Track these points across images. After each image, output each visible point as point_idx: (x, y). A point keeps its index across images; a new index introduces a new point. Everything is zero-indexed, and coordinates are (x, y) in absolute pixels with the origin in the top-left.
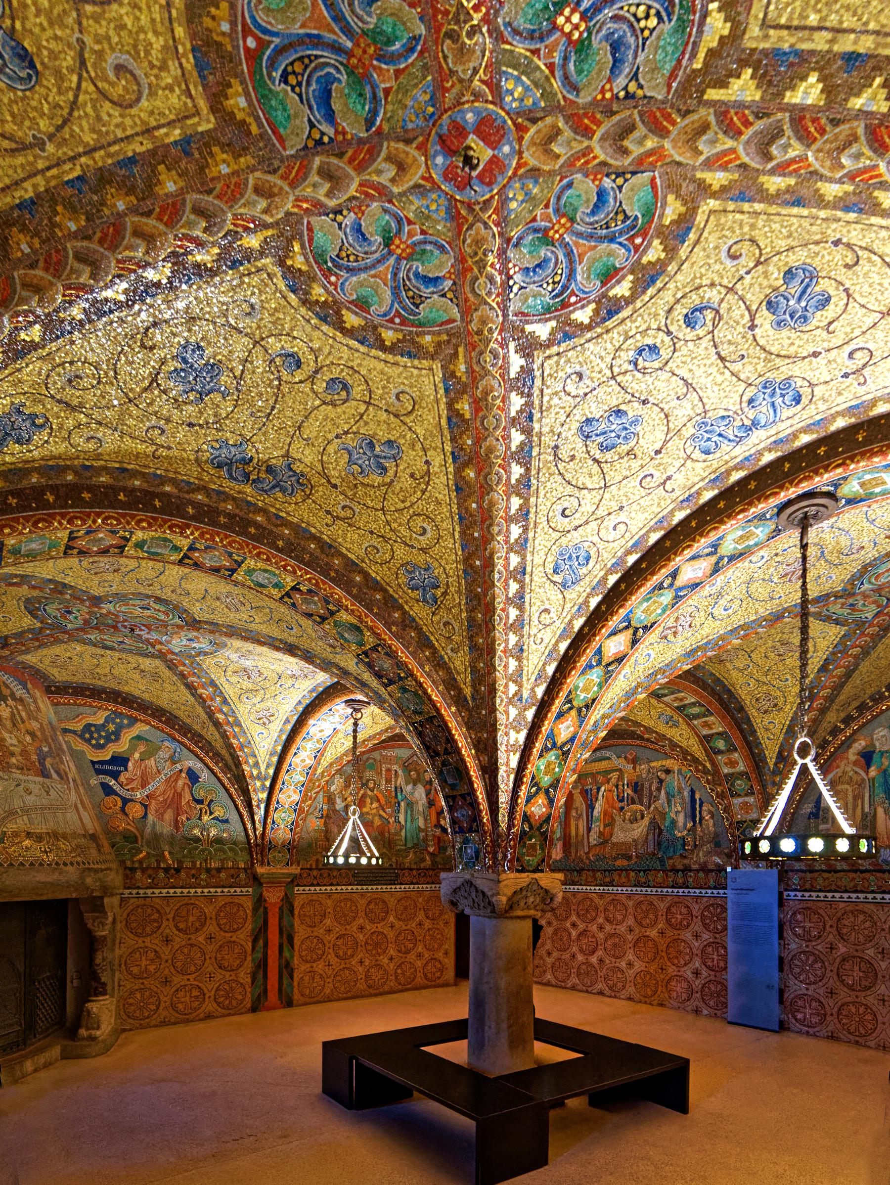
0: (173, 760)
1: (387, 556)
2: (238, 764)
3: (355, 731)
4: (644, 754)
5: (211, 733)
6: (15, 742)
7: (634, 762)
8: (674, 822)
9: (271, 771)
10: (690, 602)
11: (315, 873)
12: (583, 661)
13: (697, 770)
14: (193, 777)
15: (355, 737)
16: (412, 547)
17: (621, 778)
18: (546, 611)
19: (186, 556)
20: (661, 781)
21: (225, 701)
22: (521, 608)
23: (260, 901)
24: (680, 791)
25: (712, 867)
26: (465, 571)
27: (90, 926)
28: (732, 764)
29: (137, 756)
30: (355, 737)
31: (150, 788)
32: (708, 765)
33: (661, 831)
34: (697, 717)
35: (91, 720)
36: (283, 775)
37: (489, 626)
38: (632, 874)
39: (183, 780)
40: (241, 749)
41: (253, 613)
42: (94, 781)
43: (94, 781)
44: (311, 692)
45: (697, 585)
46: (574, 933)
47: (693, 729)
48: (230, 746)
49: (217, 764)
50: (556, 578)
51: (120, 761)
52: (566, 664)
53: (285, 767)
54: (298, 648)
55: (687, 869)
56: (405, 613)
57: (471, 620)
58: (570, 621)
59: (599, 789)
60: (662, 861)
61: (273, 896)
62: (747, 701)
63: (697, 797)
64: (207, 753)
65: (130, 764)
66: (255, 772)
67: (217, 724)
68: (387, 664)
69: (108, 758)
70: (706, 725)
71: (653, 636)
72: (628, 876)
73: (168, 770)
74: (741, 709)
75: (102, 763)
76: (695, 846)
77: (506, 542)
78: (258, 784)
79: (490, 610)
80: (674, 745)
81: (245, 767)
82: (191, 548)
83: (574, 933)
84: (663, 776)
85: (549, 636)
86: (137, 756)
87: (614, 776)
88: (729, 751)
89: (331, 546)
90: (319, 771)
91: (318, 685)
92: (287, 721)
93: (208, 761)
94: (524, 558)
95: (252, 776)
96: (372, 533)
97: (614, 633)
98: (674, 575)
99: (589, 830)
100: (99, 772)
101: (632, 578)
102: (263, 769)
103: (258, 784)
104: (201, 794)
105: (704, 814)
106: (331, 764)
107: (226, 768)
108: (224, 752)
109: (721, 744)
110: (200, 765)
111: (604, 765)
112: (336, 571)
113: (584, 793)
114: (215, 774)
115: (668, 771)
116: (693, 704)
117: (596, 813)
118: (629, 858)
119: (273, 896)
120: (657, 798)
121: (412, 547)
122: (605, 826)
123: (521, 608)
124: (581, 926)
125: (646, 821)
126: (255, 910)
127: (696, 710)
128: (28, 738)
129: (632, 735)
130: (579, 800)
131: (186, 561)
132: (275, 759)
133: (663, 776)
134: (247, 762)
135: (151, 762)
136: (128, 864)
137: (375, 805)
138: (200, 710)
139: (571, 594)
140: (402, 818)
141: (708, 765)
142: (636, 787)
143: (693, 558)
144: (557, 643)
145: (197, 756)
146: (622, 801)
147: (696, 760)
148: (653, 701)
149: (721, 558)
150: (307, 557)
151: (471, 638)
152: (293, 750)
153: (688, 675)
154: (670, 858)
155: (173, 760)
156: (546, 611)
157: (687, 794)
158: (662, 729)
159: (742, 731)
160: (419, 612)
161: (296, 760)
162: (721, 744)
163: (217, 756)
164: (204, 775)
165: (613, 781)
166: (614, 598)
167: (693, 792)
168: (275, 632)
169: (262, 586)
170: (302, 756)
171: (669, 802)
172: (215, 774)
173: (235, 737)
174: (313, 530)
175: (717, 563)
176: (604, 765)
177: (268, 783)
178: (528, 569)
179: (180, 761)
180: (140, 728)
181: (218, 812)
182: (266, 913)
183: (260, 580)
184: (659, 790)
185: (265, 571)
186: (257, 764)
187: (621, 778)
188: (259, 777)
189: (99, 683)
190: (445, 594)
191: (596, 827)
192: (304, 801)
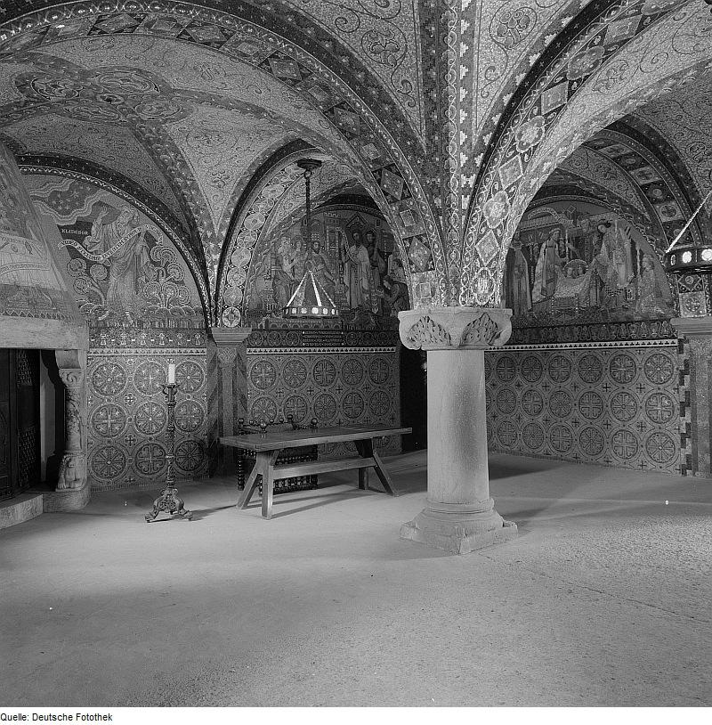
1: (354, 26)
2: (193, 227)
3: (308, 190)
4: (583, 208)
5: (169, 199)
7: (576, 216)
8: (616, 275)
9: (224, 233)
10: (619, 57)
11: (265, 334)
12: (524, 111)
13: (636, 221)
14: (151, 241)
15: (308, 195)
16: (377, 17)
17: (562, 233)
18: (493, 68)
19: (185, 32)
20: (601, 235)
21: (184, 165)
22: (470, 67)
23: (214, 361)
24: (621, 244)
25: (652, 317)
26: (422, 36)
27: (64, 380)
28: (670, 212)
29: (99, 221)
30: (308, 195)
31: (112, 251)
32: (646, 215)
33: (603, 284)
34: (634, 167)
35: (57, 188)
36: (236, 237)
37: (441, 83)
38: (576, 329)
39: (141, 244)
41: (226, 80)
42: (61, 246)
44: (264, 154)
45: (625, 41)
46: (519, 394)
47: (630, 179)
48: (185, 209)
50: (500, 40)
51: (84, 225)
52: (509, 114)
53: (238, 228)
54: (264, 110)
55: (629, 321)
56: (367, 73)
57: (427, 79)
58: (513, 76)
59: (540, 246)
60: (604, 313)
61: (227, 357)
62: (682, 150)
63: (638, 248)
64: (163, 217)
65: (93, 229)
66: (209, 234)
67: (175, 188)
68: (349, 119)
70: (642, 174)
71: (588, 88)
72: (571, 332)
74: (676, 159)
75: (67, 227)
76: (637, 297)
77: (458, 11)
78: (212, 245)
79: (443, 68)
80: (613, 197)
81: (200, 229)
82: (191, 26)
83: (519, 394)
84: (602, 229)
85: (495, 91)
86: (99, 221)
87: (555, 232)
88: (667, 200)
89: (306, 19)
90: (268, 232)
91: (272, 147)
92: (240, 183)
93: (164, 224)
94: (472, 24)
96: (342, 6)
97: (552, 85)
98: (603, 34)
99: (532, 287)
100: (65, 236)
101: (566, 37)
102: (216, 231)
103: (212, 245)
104: (157, 257)
105: (645, 264)
106: (280, 225)
107: (181, 232)
108: (181, 217)
109: (658, 194)
111: (544, 221)
112: (309, 40)
113: (526, 250)
114: (171, 238)
115: (608, 225)
116: (630, 154)
117: (538, 270)
118: (571, 313)
119: (227, 357)
120: (598, 252)
121: (377, 17)
122: (548, 282)
123: (470, 67)
124: (526, 386)
125: (588, 275)
126: (210, 371)
127: (631, 161)
128: (11, 202)
129: (573, 190)
130: (521, 258)
131: (184, 36)
132: (228, 221)
133: (602, 229)
134: (202, 224)
135: (112, 227)
136: (94, 324)
137: (320, 267)
138: (160, 176)
139: (513, 54)
140: (346, 280)
141: (646, 215)
142: (578, 241)
143: (619, 19)
144: (501, 96)
145: (154, 220)
146: (564, 256)
147: (634, 211)
148: (591, 153)
149: (645, 17)
150: (285, 29)
151: (426, 93)
152: (246, 212)
153: (618, 126)
154: (612, 310)
156: (493, 68)
157: (627, 245)
158: (601, 182)
159: (678, 180)
160: (380, 72)
161: (249, 221)
162: (658, 194)
163: (172, 220)
164: (161, 239)
165: (555, 236)
166: (550, 55)
167: (633, 243)
168: (245, 97)
169: (245, 55)
170: (254, 219)
171: (610, 255)
172: (171, 238)
174: (292, 6)
175: (642, 22)
176: (544, 221)
177: (221, 245)
178: (476, 33)
180: (101, 195)
181: (175, 274)
182: (220, 373)
183: (244, 50)
184: (600, 243)
185: (250, 42)
186: (211, 226)
187: (562, 233)
188: (213, 239)
189: (66, 153)
190: (404, 56)
191: (538, 286)
192: (255, 261)
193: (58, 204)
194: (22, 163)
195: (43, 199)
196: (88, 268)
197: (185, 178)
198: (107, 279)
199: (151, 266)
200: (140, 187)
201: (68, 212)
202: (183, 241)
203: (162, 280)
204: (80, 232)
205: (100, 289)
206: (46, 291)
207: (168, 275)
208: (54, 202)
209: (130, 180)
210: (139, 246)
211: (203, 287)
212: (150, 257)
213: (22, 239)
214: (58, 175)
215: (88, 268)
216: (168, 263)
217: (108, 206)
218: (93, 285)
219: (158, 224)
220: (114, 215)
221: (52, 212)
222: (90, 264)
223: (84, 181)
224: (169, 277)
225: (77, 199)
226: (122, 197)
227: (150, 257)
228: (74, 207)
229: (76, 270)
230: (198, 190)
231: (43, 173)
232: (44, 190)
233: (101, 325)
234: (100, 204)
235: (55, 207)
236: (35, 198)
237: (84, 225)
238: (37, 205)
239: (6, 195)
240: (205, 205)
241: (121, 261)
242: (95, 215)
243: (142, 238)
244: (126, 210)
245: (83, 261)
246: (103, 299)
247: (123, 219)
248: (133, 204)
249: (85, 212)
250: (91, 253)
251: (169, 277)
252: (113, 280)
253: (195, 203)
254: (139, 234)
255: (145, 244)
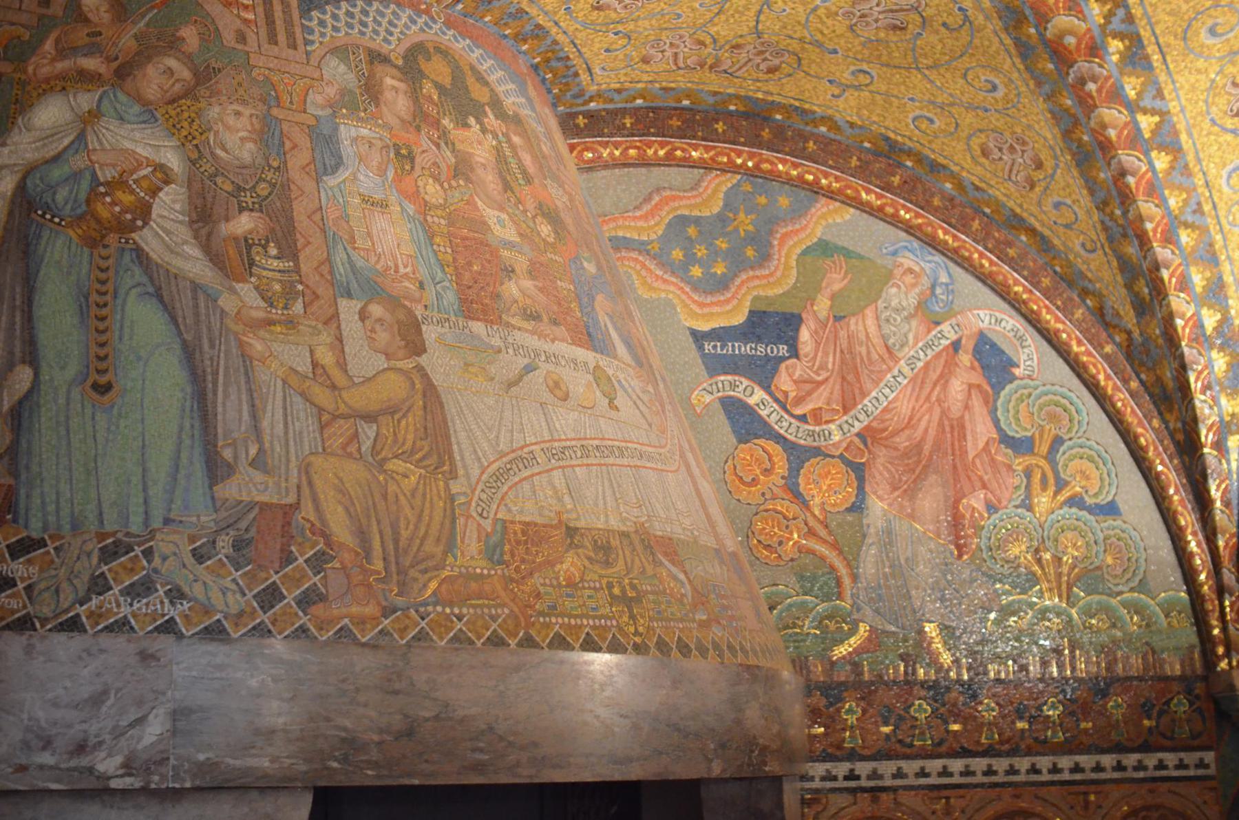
0: (929, 314)
6: (510, 234)
14: (993, 363)
29: (823, 306)
40: (1169, 239)
42: (705, 395)
43: (705, 395)
49: (1067, 310)
65: (805, 335)
66: (1210, 320)
69: (739, 319)
73: (918, 349)
81: (1179, 302)
86: (823, 306)
95: (1199, 337)
100: (717, 365)
110: (1011, 322)
128: (545, 229)
134: (1184, 284)
145: (1003, 292)
155: (929, 314)
164: (1030, 355)
173: (1153, 191)
179: (950, 313)
193: (690, 259)
194: (577, 131)
195: (642, 248)
196: (794, 471)
197: (1133, 107)
198: (857, 507)
199: (1003, 455)
200: (954, 177)
201: (722, 284)
202: (1107, 357)
203: (1043, 501)
204: (761, 349)
205: (835, 546)
206: (669, 548)
207: (1061, 485)
208: (677, 254)
209: (919, 159)
210: (957, 386)
211: (1187, 519)
212: (996, 423)
213: (582, 354)
214: (687, 163)
215: (794, 471)
216: (1057, 441)
217: (847, 253)
218: (811, 533)
219: (1017, 305)
220: (871, 281)
221: (669, 291)
222: (798, 455)
223: (773, 176)
224: (1066, 494)
225: (752, 239)
226: (894, 221)
227: (996, 423)
228: (738, 264)
229: (755, 482)
230: (1175, 150)
231: (644, 163)
232: (645, 217)
233: (842, 675)
234: (824, 248)
235: (680, 270)
236: (620, 244)
237: (774, 326)
238: (631, 268)
239: (531, 205)
240: (1199, 210)
241: (902, 441)
242: (809, 285)
243: (965, 358)
244: (907, 263)
245: (775, 449)
246: (847, 581)
247: (900, 296)
248: (932, 243)
249: (774, 284)
250: (802, 418)
251: (1066, 494)
252: (878, 507)
253: (1162, 203)
254: (956, 346)
255: (976, 378)
